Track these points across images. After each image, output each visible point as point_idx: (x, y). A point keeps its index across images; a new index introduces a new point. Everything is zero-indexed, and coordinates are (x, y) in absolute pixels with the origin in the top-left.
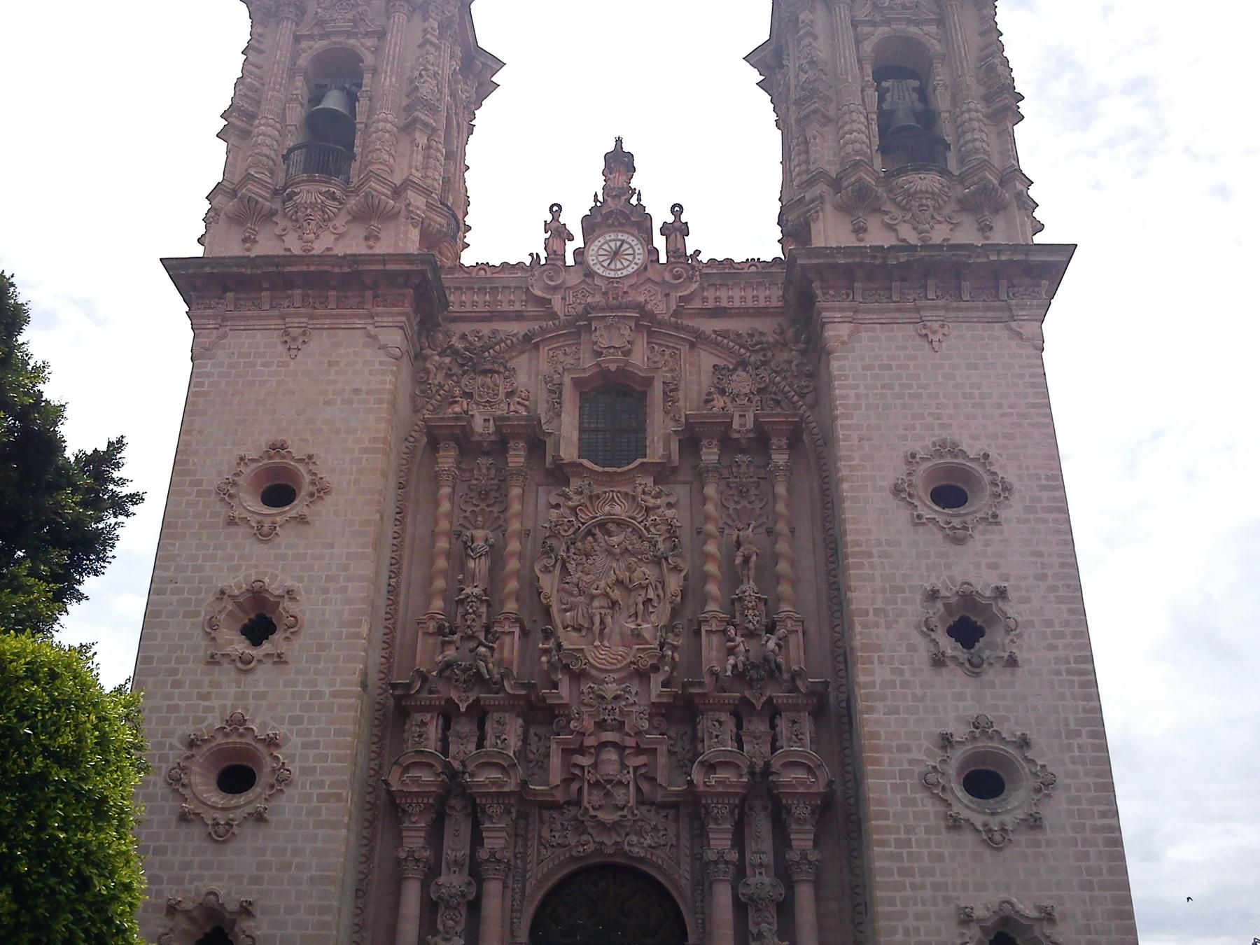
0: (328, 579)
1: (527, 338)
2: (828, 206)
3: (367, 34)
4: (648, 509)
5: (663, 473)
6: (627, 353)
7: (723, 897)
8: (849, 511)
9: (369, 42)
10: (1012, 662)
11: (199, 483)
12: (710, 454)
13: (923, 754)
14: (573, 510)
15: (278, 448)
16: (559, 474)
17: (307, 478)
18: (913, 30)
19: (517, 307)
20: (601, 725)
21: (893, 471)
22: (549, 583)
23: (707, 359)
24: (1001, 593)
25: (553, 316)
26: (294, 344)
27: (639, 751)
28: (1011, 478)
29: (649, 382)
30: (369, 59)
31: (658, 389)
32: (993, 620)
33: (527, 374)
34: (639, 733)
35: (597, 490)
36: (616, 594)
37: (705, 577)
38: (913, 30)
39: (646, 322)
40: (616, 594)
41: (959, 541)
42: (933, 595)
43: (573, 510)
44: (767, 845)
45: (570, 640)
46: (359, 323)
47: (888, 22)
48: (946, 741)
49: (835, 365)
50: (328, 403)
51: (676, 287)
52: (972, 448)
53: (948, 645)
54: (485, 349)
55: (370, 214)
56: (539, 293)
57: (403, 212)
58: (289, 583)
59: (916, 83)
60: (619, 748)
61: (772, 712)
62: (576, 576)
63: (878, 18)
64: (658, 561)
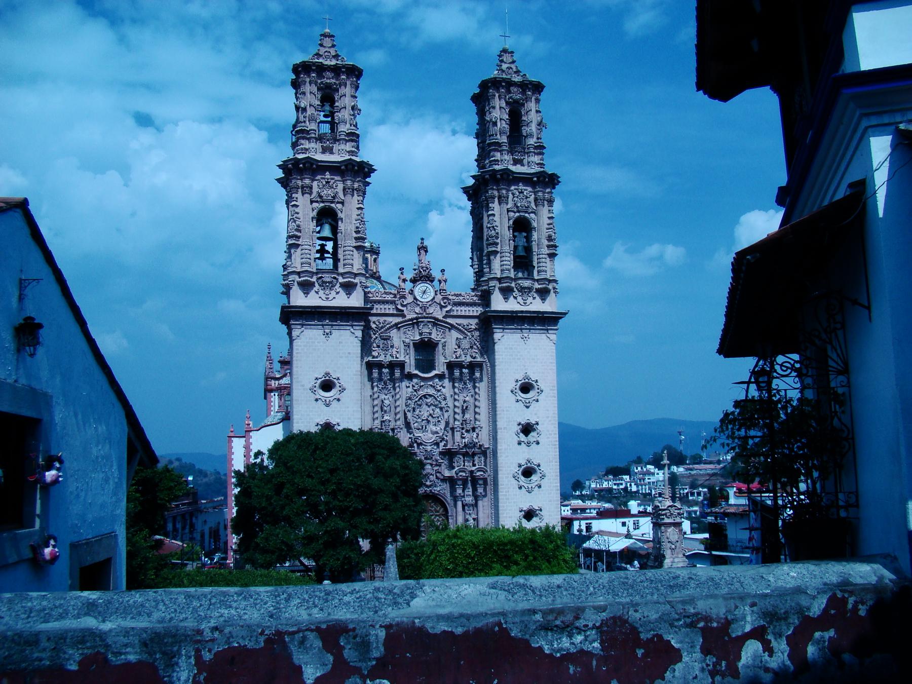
0: (349, 418)
1: (396, 325)
2: (497, 289)
3: (338, 203)
4: (439, 391)
5: (441, 377)
6: (430, 334)
7: (459, 504)
8: (499, 397)
9: (339, 206)
10: (538, 443)
11: (303, 386)
12: (457, 373)
13: (515, 469)
14: (415, 391)
15: (327, 374)
16: (410, 377)
17: (338, 385)
18: (527, 215)
19: (391, 312)
20: (426, 458)
21: (512, 385)
22: (409, 415)
23: (455, 334)
24: (537, 424)
25: (404, 316)
26: (327, 335)
27: (436, 465)
28: (542, 388)
29: (437, 344)
30: (340, 215)
31: (440, 346)
32: (534, 430)
33: (396, 337)
34: (437, 461)
35: (422, 384)
36: (430, 418)
37: (455, 413)
38: (527, 215)
39: (436, 323)
40: (430, 418)
41: (527, 407)
42: (519, 424)
43: (415, 391)
44: (471, 490)
45: (418, 434)
46: (348, 328)
47: (519, 212)
48: (520, 466)
49: (496, 347)
50: (341, 357)
51: (445, 307)
52: (534, 377)
53: (522, 435)
54: (382, 327)
55: (349, 288)
56: (399, 307)
57: (359, 285)
58: (339, 421)
59: (525, 234)
60: (431, 465)
61: (474, 454)
62: (417, 412)
63: (515, 210)
64: (441, 409)
